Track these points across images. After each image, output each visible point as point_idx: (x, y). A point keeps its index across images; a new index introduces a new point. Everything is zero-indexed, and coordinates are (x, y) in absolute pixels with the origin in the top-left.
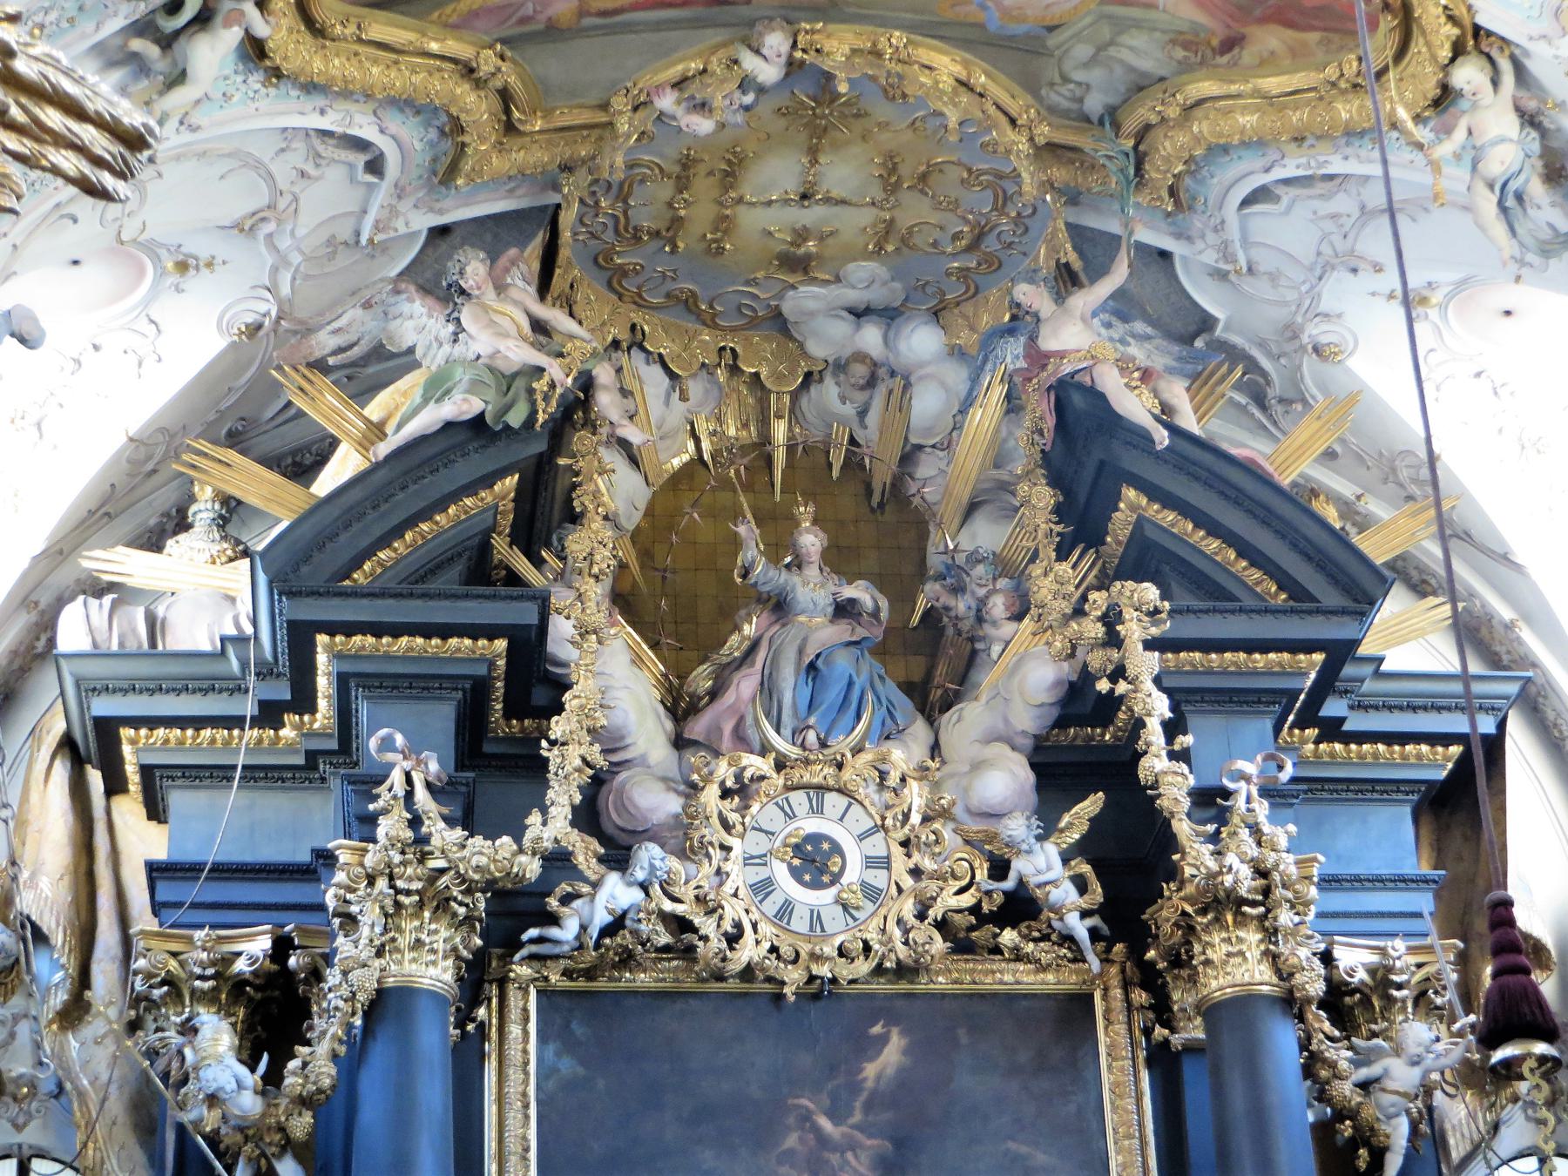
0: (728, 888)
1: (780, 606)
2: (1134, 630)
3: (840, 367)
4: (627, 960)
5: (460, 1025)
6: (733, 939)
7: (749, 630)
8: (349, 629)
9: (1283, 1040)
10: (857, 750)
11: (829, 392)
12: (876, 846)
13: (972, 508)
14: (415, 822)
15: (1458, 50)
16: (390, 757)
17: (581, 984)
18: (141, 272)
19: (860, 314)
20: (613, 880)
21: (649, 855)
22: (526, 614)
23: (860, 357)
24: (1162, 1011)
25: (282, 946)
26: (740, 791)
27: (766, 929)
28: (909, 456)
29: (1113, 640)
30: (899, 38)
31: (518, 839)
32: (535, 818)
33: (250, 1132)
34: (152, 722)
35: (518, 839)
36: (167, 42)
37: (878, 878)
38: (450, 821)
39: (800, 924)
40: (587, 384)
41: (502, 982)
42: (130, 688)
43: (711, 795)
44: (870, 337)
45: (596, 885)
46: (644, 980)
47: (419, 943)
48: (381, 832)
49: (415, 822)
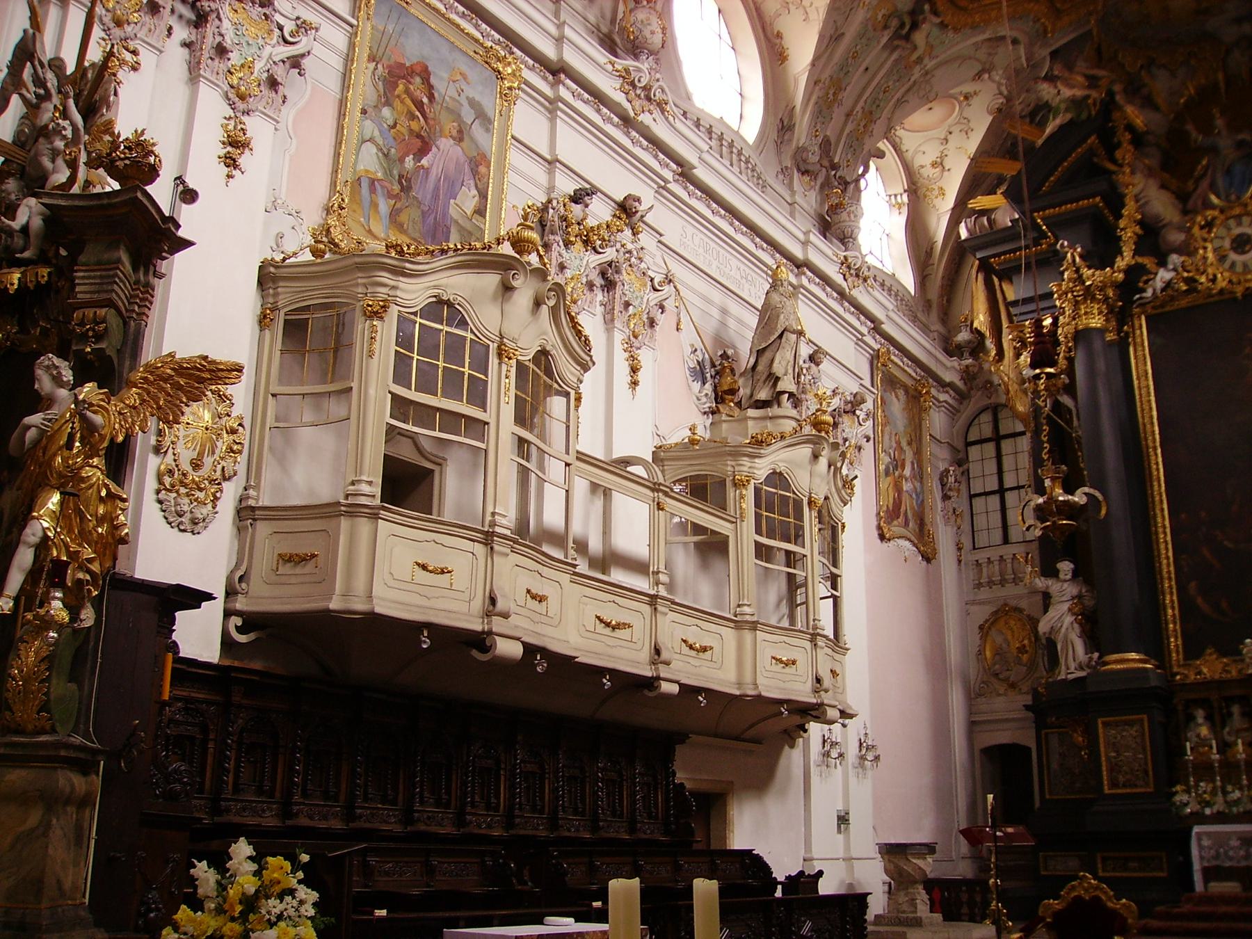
0: (1209, 261)
1: (1214, 150)
4: (1172, 299)
5: (1118, 334)
6: (1214, 280)
7: (1204, 162)
8: (1044, 209)
16: (1066, 249)
17: (1160, 311)
18: (953, 104)
21: (1175, 259)
26: (1209, 225)
27: (1226, 274)
31: (1112, 268)
32: (1119, 259)
34: (999, 255)
35: (1112, 268)
38: (1089, 268)
39: (1239, 269)
40: (1111, 94)
41: (1132, 316)
46: (1183, 303)
47: (1086, 313)
48: (1066, 276)
49: (1077, 271)
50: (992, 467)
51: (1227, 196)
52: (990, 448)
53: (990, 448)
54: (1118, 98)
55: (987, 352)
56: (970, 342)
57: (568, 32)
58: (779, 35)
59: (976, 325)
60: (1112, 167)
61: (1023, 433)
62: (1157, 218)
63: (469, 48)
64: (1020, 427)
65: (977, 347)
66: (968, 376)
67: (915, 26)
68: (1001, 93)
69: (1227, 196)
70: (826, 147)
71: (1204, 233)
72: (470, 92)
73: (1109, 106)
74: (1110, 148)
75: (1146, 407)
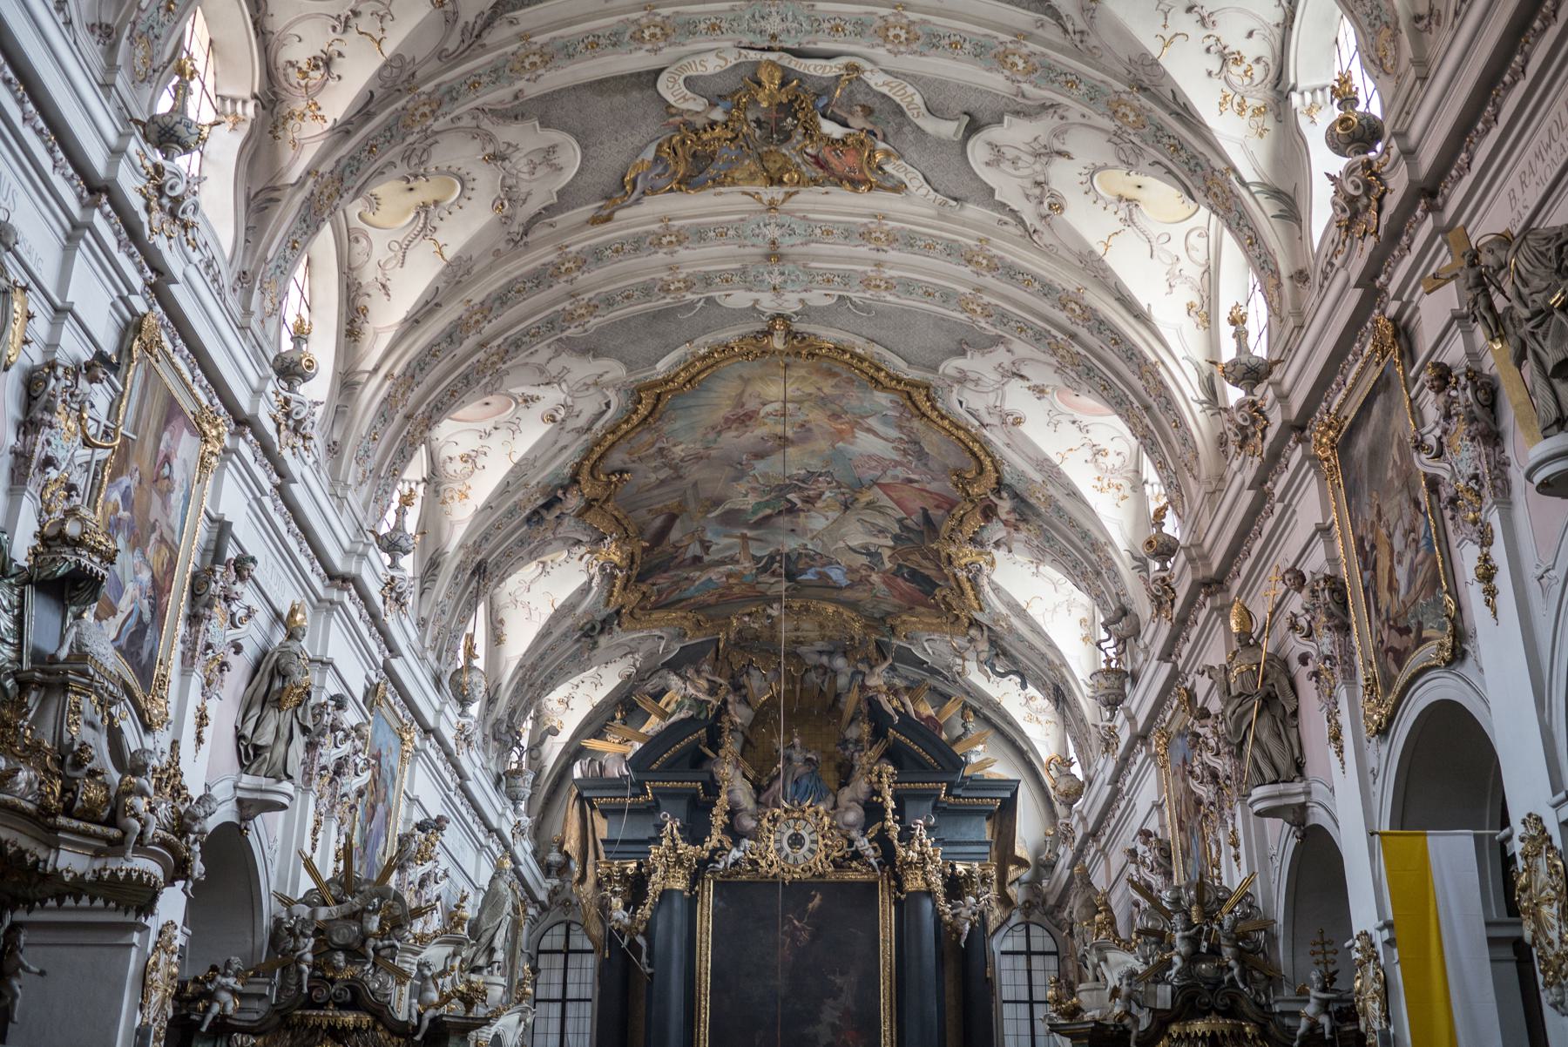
2: (885, 780)
3: (816, 667)
4: (738, 873)
6: (770, 866)
9: (927, 905)
10: (811, 806)
11: (813, 675)
12: (814, 836)
13: (853, 720)
14: (673, 840)
15: (971, 624)
19: (821, 653)
20: (734, 851)
21: (746, 843)
22: (707, 777)
23: (822, 666)
24: (900, 887)
25: (640, 866)
26: (775, 820)
28: (837, 697)
29: (880, 782)
30: (814, 602)
33: (628, 928)
36: (591, 637)
37: (814, 847)
38: (683, 839)
39: (791, 861)
40: (725, 702)
42: (594, 788)
43: (765, 822)
44: (825, 660)
45: (729, 851)
49: (673, 840)
50: (557, 977)
51: (792, 800)
52: (560, 958)
53: (560, 958)
54: (730, 707)
55: (571, 873)
56: (559, 863)
57: (447, 709)
58: (501, 622)
59: (566, 847)
60: (712, 755)
61: (591, 952)
62: (737, 804)
63: (396, 725)
64: (589, 946)
65: (563, 869)
66: (554, 893)
67: (602, 631)
68: (634, 665)
69: (792, 800)
70: (511, 716)
71: (770, 826)
72: (392, 763)
73: (722, 710)
74: (714, 742)
75: (704, 959)
